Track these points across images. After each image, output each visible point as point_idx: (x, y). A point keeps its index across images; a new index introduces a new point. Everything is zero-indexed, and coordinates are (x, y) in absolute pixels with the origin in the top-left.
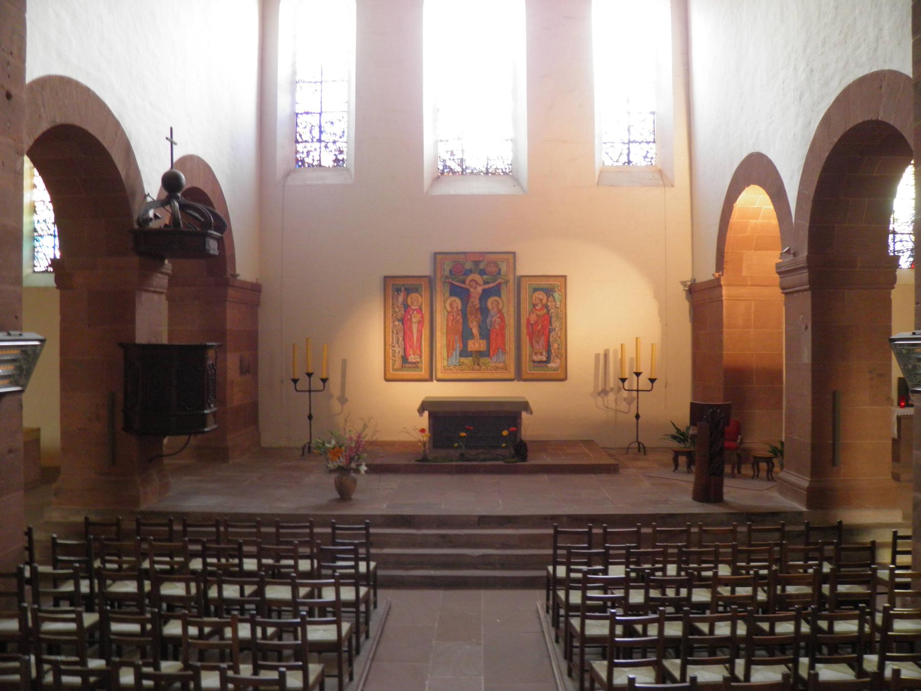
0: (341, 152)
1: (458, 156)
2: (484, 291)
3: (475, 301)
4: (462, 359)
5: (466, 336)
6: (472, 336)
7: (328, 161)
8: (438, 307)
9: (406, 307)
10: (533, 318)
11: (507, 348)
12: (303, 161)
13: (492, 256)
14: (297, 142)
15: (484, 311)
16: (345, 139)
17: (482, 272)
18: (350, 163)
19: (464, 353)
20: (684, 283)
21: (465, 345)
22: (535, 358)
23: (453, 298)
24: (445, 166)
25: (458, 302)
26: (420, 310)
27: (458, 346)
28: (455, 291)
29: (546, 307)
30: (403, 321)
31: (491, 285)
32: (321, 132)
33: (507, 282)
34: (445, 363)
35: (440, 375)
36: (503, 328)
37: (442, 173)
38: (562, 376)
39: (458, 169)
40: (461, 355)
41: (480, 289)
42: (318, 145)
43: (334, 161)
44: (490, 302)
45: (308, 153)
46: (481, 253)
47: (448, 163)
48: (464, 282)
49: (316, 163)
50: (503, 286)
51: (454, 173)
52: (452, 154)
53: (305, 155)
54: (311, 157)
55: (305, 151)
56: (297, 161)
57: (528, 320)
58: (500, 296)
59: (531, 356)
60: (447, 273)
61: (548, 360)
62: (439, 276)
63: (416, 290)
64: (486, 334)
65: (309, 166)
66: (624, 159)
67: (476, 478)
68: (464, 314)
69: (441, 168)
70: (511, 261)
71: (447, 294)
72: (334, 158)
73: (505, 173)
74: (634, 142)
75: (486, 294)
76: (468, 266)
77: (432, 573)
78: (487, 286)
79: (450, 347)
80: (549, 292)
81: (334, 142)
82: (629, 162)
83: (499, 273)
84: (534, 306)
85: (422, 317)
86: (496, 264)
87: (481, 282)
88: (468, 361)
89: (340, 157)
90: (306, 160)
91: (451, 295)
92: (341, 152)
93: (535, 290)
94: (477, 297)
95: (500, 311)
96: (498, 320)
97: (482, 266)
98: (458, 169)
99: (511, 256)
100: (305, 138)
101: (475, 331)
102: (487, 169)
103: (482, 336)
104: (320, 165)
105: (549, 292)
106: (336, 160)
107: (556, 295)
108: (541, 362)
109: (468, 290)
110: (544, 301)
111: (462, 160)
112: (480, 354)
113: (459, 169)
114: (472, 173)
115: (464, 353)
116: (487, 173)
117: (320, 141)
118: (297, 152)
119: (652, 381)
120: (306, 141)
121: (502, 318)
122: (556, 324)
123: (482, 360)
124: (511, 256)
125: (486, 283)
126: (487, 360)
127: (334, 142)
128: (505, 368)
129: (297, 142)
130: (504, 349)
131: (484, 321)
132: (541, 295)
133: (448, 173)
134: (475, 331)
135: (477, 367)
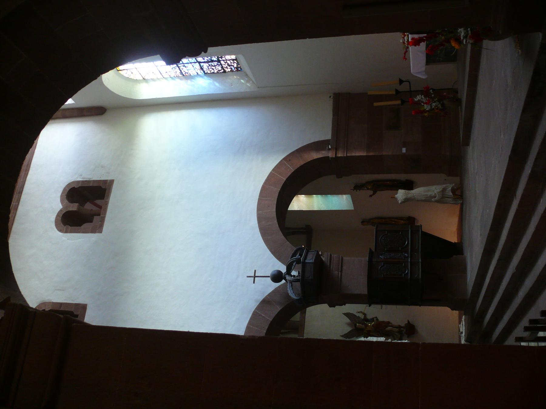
12: (237, 68)
54: (232, 64)
56: (238, 70)
100: (220, 69)
104: (236, 60)
117: (219, 61)
118: (232, 71)
120: (222, 67)
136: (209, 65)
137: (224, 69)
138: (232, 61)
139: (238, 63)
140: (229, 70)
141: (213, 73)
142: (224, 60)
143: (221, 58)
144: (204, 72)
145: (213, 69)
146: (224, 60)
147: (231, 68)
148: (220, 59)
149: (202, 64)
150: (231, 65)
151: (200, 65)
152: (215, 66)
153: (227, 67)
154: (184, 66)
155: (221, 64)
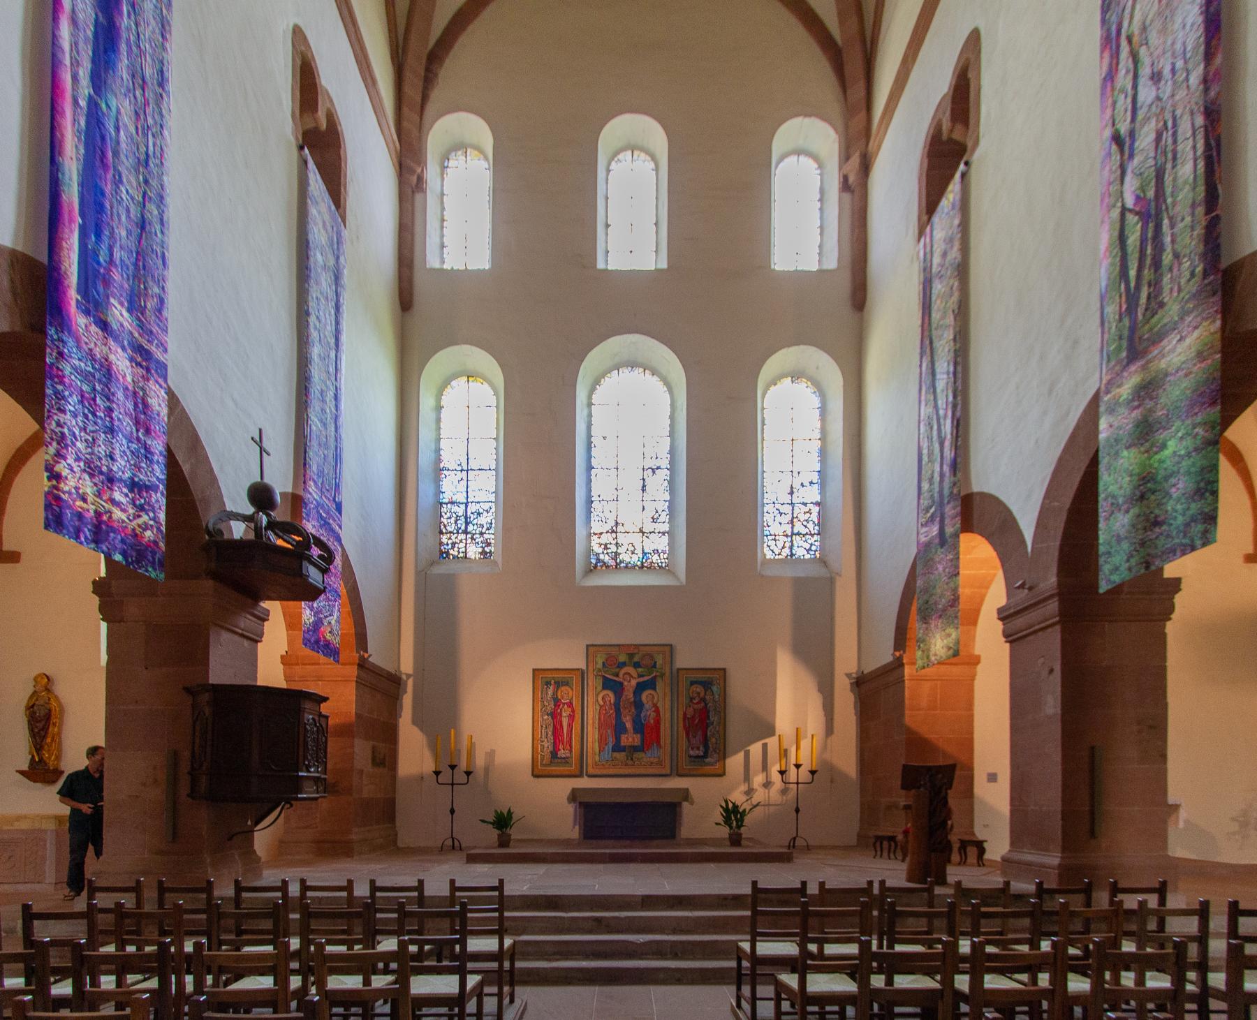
0: (489, 545)
1: (613, 548)
2: (638, 684)
3: (629, 694)
4: (615, 754)
5: (619, 729)
6: (625, 730)
7: (473, 552)
8: (590, 699)
9: (557, 703)
10: (690, 713)
11: (662, 743)
12: (447, 553)
13: (647, 649)
15: (638, 705)
16: (492, 531)
17: (637, 665)
19: (617, 748)
20: (848, 675)
21: (618, 739)
22: (692, 753)
23: (606, 692)
24: (598, 560)
25: (611, 696)
26: (570, 704)
27: (611, 741)
28: (607, 684)
29: (703, 700)
30: (555, 715)
31: (646, 678)
32: (467, 524)
33: (662, 675)
34: (597, 758)
35: (591, 771)
36: (658, 721)
37: (595, 567)
38: (720, 772)
39: (612, 563)
40: (614, 750)
41: (634, 682)
42: (463, 536)
44: (645, 696)
45: (454, 544)
46: (637, 646)
47: (602, 557)
48: (617, 675)
50: (659, 679)
51: (608, 567)
52: (606, 548)
56: (441, 553)
57: (685, 714)
58: (654, 689)
59: (687, 750)
60: (600, 665)
61: (705, 756)
62: (591, 668)
63: (567, 683)
64: (639, 727)
66: (786, 552)
67: (632, 866)
68: (617, 706)
69: (594, 561)
70: (668, 653)
71: (600, 688)
74: (798, 534)
75: (641, 688)
76: (622, 658)
77: (584, 964)
78: (641, 680)
79: (602, 741)
80: (707, 685)
81: (482, 534)
82: (792, 555)
83: (654, 666)
84: (691, 699)
85: (573, 711)
86: (652, 657)
87: (635, 675)
88: (621, 756)
90: (451, 552)
91: (604, 688)
92: (489, 545)
93: (692, 683)
94: (631, 690)
95: (655, 705)
96: (653, 715)
97: (636, 659)
98: (612, 563)
99: (667, 649)
100: (449, 529)
101: (629, 725)
103: (636, 731)
105: (707, 685)
106: (483, 553)
107: (715, 688)
108: (698, 757)
109: (621, 684)
110: (702, 694)
112: (635, 749)
114: (626, 567)
115: (617, 748)
116: (642, 567)
117: (466, 532)
118: (441, 543)
119: (813, 772)
121: (657, 711)
122: (714, 718)
123: (636, 755)
124: (667, 649)
125: (640, 676)
126: (640, 755)
127: (482, 534)
128: (660, 763)
129: (441, 532)
130: (658, 743)
131: (638, 715)
132: (699, 689)
134: (629, 725)
135: (630, 762)
143: (472, 538)
149: (463, 507)
150: (453, 548)
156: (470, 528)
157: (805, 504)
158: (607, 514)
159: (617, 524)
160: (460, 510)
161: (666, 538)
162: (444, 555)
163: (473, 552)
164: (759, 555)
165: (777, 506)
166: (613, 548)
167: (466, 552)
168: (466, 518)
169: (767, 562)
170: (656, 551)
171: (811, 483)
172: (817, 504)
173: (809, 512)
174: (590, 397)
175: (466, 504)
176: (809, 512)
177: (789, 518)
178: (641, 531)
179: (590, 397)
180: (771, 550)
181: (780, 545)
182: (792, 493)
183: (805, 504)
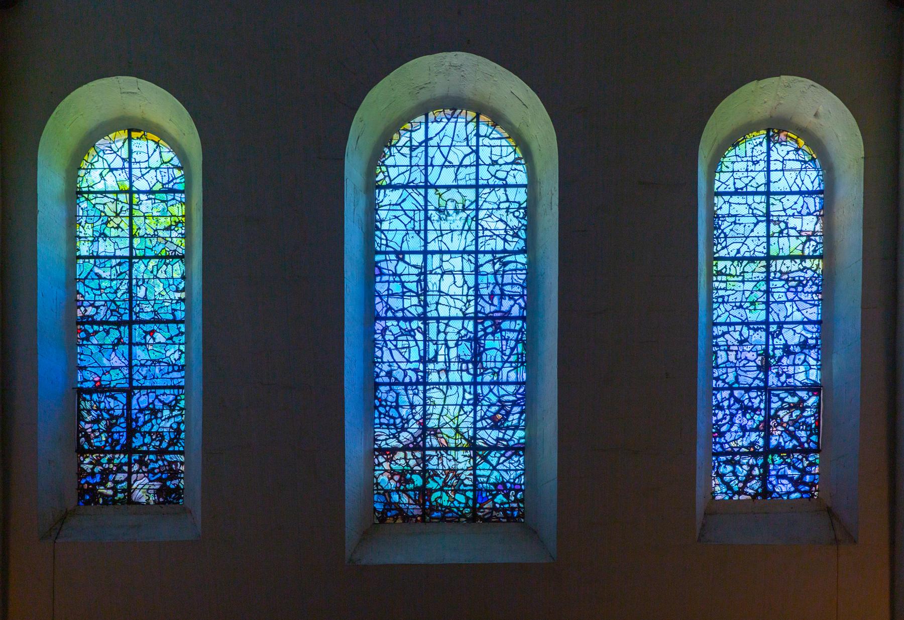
0: (174, 474)
1: (418, 481)
7: (143, 489)
12: (93, 491)
14: (81, 451)
18: (194, 498)
24: (389, 505)
32: (131, 432)
39: (416, 510)
42: (123, 458)
43: (158, 492)
45: (105, 473)
47: (395, 497)
49: (120, 496)
51: (405, 517)
53: (98, 479)
54: (110, 484)
55: (98, 469)
65: (105, 503)
72: (157, 485)
73: (510, 519)
74: (779, 450)
82: (766, 493)
89: (171, 484)
90: (102, 490)
92: (174, 474)
98: (416, 510)
100: (96, 443)
102: (474, 510)
104: (129, 501)
111: (424, 492)
113: (419, 512)
114: (443, 519)
116: (474, 518)
117: (128, 449)
118: (81, 472)
120: (100, 450)
127: (160, 452)
133: (395, 518)
136: (112, 417)
137: (92, 452)
138: (125, 485)
139: (115, 502)
140: (88, 467)
141: (81, 418)
142: (129, 464)
143: (141, 462)
144: (90, 391)
145: (96, 421)
146: (129, 464)
147: (93, 474)
148: (136, 457)
149: (122, 398)
150: (103, 483)
151: (121, 390)
152: (108, 430)
153: (98, 463)
154: (119, 341)
155: (113, 452)
156: (137, 442)
157: (792, 390)
158: (404, 412)
159: (424, 428)
160: (116, 405)
161: (517, 461)
162: (88, 495)
163: (143, 489)
164: (700, 491)
165: (737, 393)
166: (418, 481)
167: (129, 491)
168: (129, 419)
169: (714, 508)
170: (501, 487)
171: (804, 345)
172: (814, 388)
173: (800, 405)
174: (371, 173)
175: (129, 392)
176: (800, 405)
177: (758, 418)
178: (472, 446)
179: (371, 173)
180: (725, 483)
181: (742, 471)
182: (765, 368)
183: (792, 390)
